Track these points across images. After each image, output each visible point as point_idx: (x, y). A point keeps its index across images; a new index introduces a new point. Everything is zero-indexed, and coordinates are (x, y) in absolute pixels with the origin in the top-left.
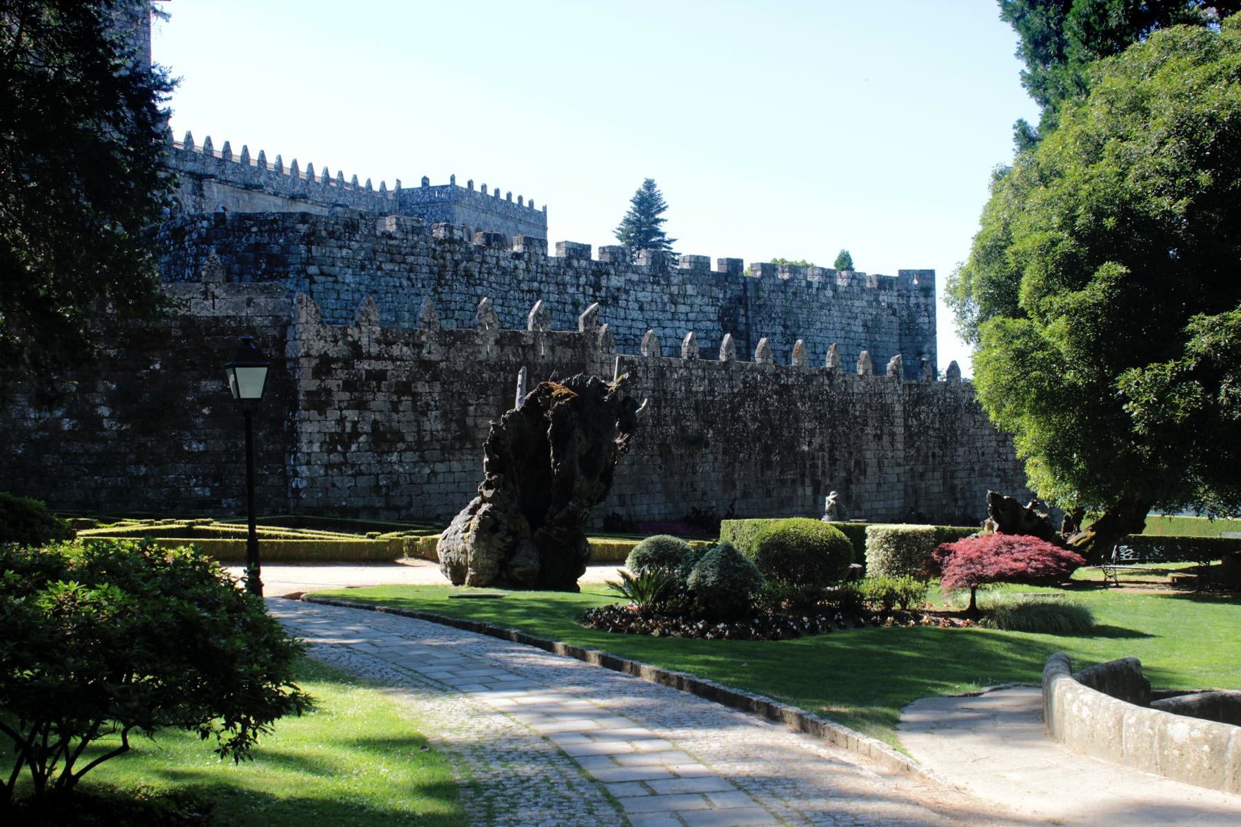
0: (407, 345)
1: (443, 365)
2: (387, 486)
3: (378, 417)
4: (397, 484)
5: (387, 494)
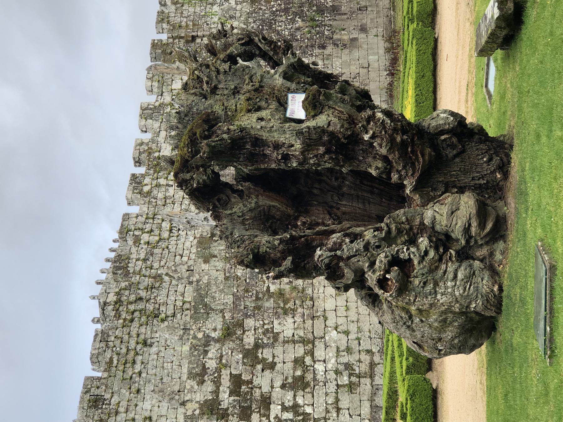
0: (206, 352)
1: (228, 315)
2: (350, 375)
3: (278, 383)
4: (348, 366)
5: (359, 376)
